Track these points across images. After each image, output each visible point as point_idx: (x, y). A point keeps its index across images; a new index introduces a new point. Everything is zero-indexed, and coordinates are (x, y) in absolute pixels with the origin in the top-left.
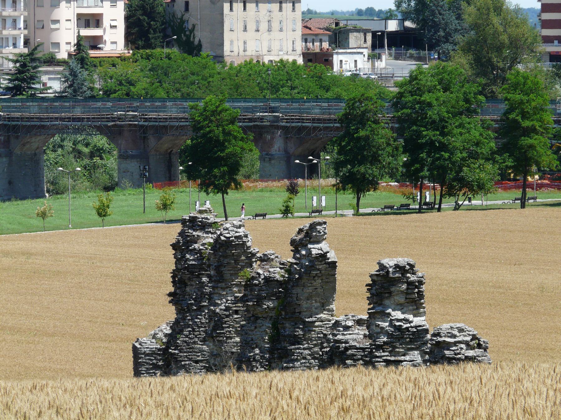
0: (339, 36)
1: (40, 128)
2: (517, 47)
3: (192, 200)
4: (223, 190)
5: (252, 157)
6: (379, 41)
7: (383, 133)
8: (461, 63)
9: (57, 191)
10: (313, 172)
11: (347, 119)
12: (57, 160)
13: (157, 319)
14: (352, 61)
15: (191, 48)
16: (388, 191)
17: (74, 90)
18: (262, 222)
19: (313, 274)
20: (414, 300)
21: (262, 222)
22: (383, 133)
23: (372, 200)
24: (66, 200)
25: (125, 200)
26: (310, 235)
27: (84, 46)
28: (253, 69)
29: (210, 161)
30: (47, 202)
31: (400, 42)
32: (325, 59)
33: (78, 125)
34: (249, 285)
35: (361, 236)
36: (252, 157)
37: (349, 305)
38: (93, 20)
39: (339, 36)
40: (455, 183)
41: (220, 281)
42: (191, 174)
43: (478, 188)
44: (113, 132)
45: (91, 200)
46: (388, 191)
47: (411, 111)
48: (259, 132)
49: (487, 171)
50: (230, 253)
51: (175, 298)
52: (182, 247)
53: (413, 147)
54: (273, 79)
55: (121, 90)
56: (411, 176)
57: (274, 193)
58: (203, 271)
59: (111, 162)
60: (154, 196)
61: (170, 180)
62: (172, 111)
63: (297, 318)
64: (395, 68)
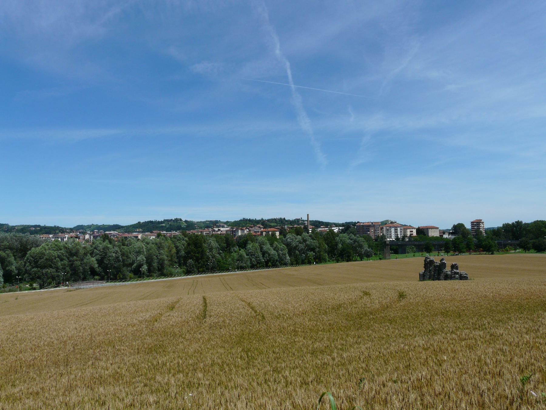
0: (444, 233)
1: (406, 245)
2: (468, 234)
3: (427, 255)
4: (429, 253)
5: (433, 248)
6: (449, 234)
7: (451, 245)
8: (460, 236)
9: (408, 253)
10: (441, 250)
11: (446, 243)
12: (408, 249)
13: (422, 270)
14: (446, 236)
15: (425, 235)
16: (452, 253)
17: (410, 240)
18: (436, 257)
19: (443, 265)
20: (457, 268)
21: (436, 257)
22: (451, 245)
23: (449, 254)
24: (409, 254)
25: (417, 254)
26: (443, 260)
27: (411, 234)
28: (433, 237)
29: (428, 250)
30: (407, 254)
31: (452, 234)
32: (442, 236)
33: (410, 245)
34: (434, 266)
35: (449, 259)
36: (433, 248)
37: (448, 270)
38: (412, 232)
39: (444, 232)
40: (461, 252)
41: (431, 265)
42: (425, 251)
43: (464, 252)
44: (415, 245)
45: (413, 254)
46: (452, 253)
47: (454, 242)
48: (434, 245)
49: (465, 250)
50: (432, 262)
51: (424, 267)
52: (425, 261)
53: (455, 247)
54: (435, 238)
55: (416, 240)
56: (455, 251)
57: (436, 253)
58: (428, 264)
59: (415, 249)
60: (421, 253)
61: (422, 251)
62: (422, 243)
63: (441, 270)
64: (452, 237)
